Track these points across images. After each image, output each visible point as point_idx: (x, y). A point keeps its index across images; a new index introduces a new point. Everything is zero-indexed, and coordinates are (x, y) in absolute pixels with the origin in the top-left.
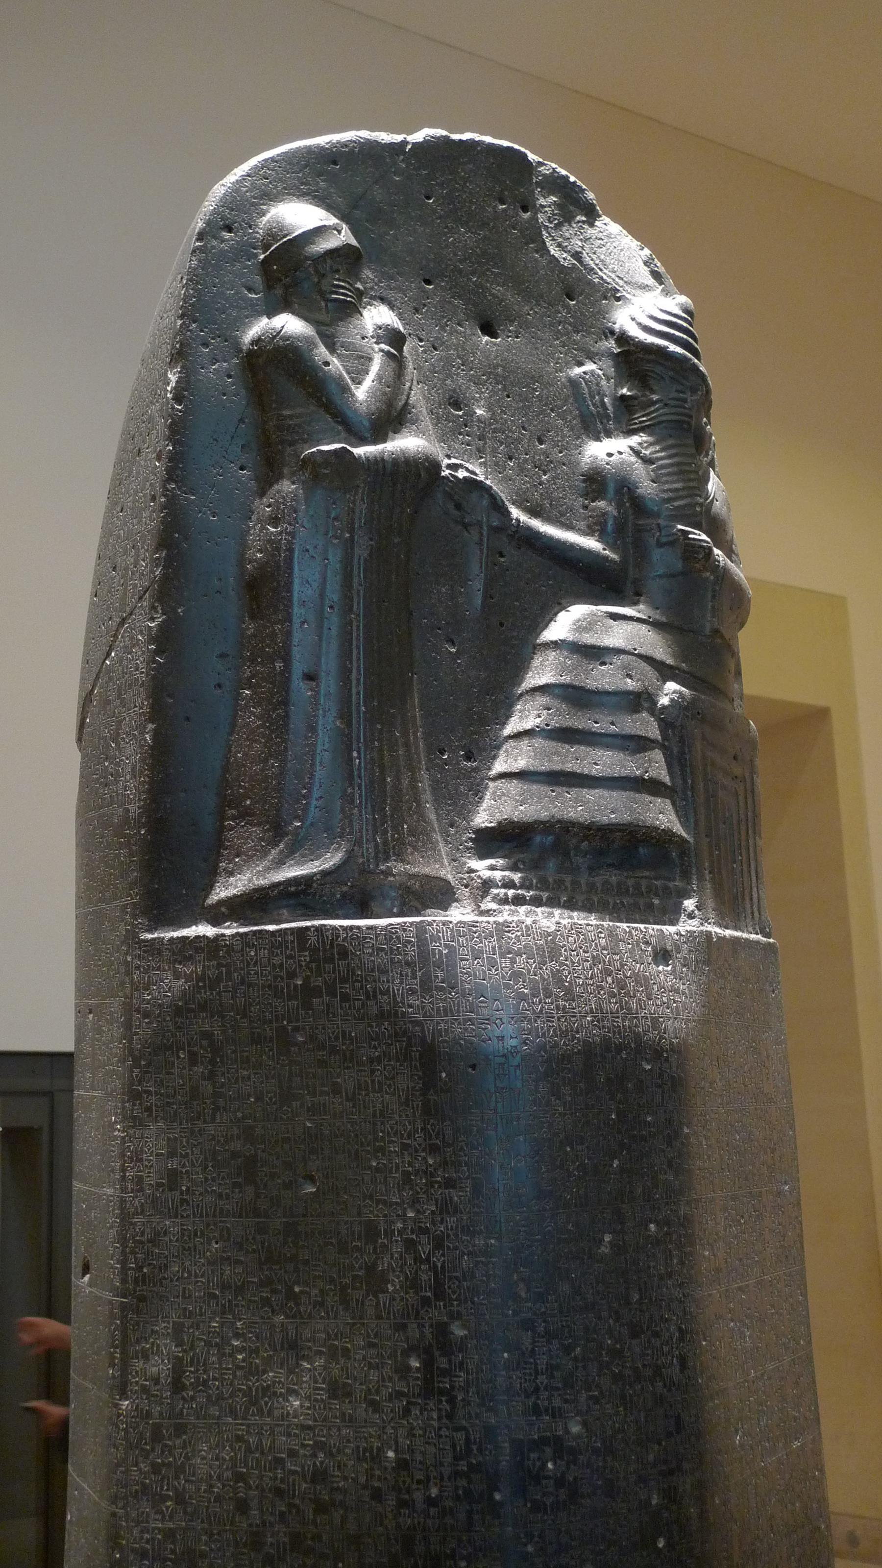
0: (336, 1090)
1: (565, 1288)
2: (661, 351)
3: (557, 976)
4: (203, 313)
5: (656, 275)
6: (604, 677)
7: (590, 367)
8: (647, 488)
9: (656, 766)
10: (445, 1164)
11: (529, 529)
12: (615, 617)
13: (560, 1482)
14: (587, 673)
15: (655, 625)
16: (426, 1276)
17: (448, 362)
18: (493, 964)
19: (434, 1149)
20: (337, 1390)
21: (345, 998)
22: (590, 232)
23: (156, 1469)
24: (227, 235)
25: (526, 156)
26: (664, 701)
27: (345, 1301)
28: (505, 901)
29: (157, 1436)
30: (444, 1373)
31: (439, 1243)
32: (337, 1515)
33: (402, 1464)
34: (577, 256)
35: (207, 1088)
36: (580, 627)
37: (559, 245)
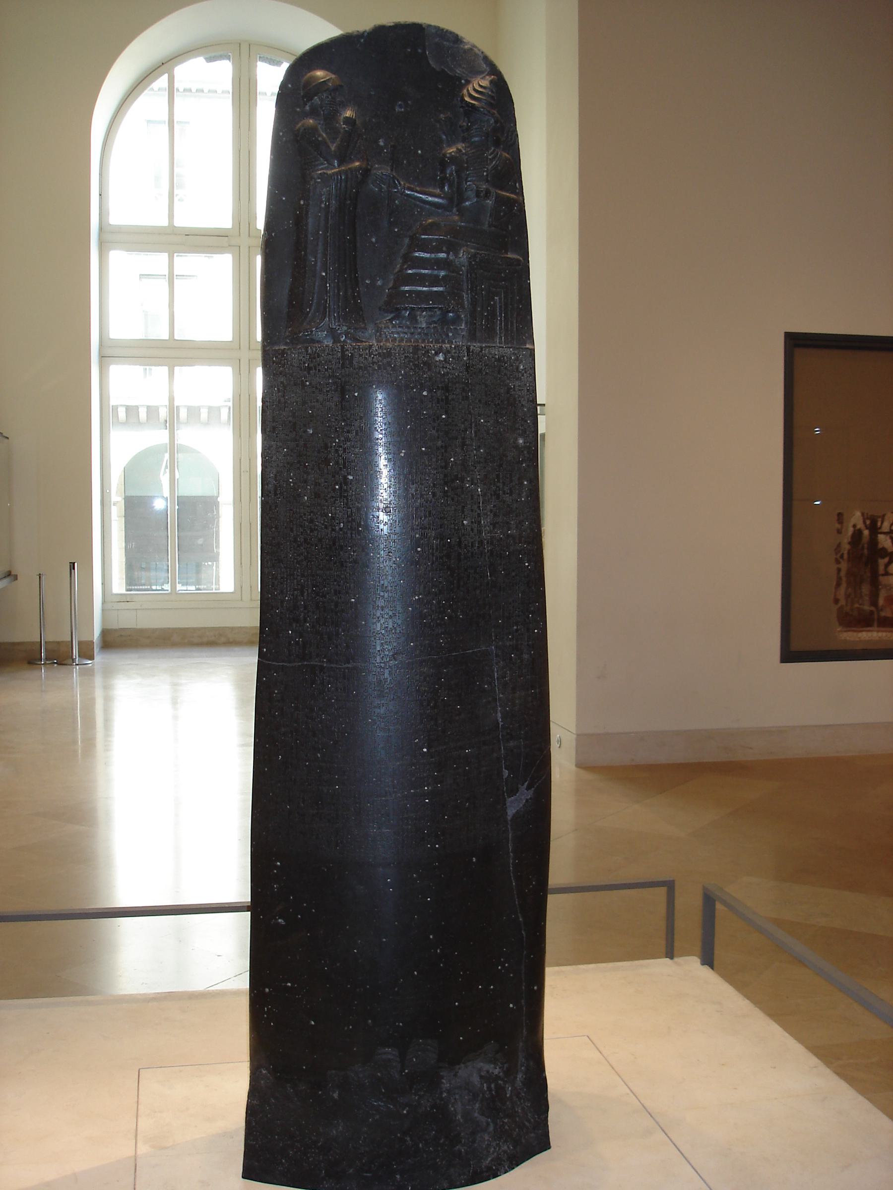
0: (317, 401)
3: (389, 364)
10: (346, 425)
16: (341, 461)
19: (344, 421)
20: (317, 495)
21: (319, 371)
23: (270, 519)
29: (270, 509)
30: (346, 491)
31: (345, 450)
32: (316, 532)
33: (333, 518)
35: (282, 399)
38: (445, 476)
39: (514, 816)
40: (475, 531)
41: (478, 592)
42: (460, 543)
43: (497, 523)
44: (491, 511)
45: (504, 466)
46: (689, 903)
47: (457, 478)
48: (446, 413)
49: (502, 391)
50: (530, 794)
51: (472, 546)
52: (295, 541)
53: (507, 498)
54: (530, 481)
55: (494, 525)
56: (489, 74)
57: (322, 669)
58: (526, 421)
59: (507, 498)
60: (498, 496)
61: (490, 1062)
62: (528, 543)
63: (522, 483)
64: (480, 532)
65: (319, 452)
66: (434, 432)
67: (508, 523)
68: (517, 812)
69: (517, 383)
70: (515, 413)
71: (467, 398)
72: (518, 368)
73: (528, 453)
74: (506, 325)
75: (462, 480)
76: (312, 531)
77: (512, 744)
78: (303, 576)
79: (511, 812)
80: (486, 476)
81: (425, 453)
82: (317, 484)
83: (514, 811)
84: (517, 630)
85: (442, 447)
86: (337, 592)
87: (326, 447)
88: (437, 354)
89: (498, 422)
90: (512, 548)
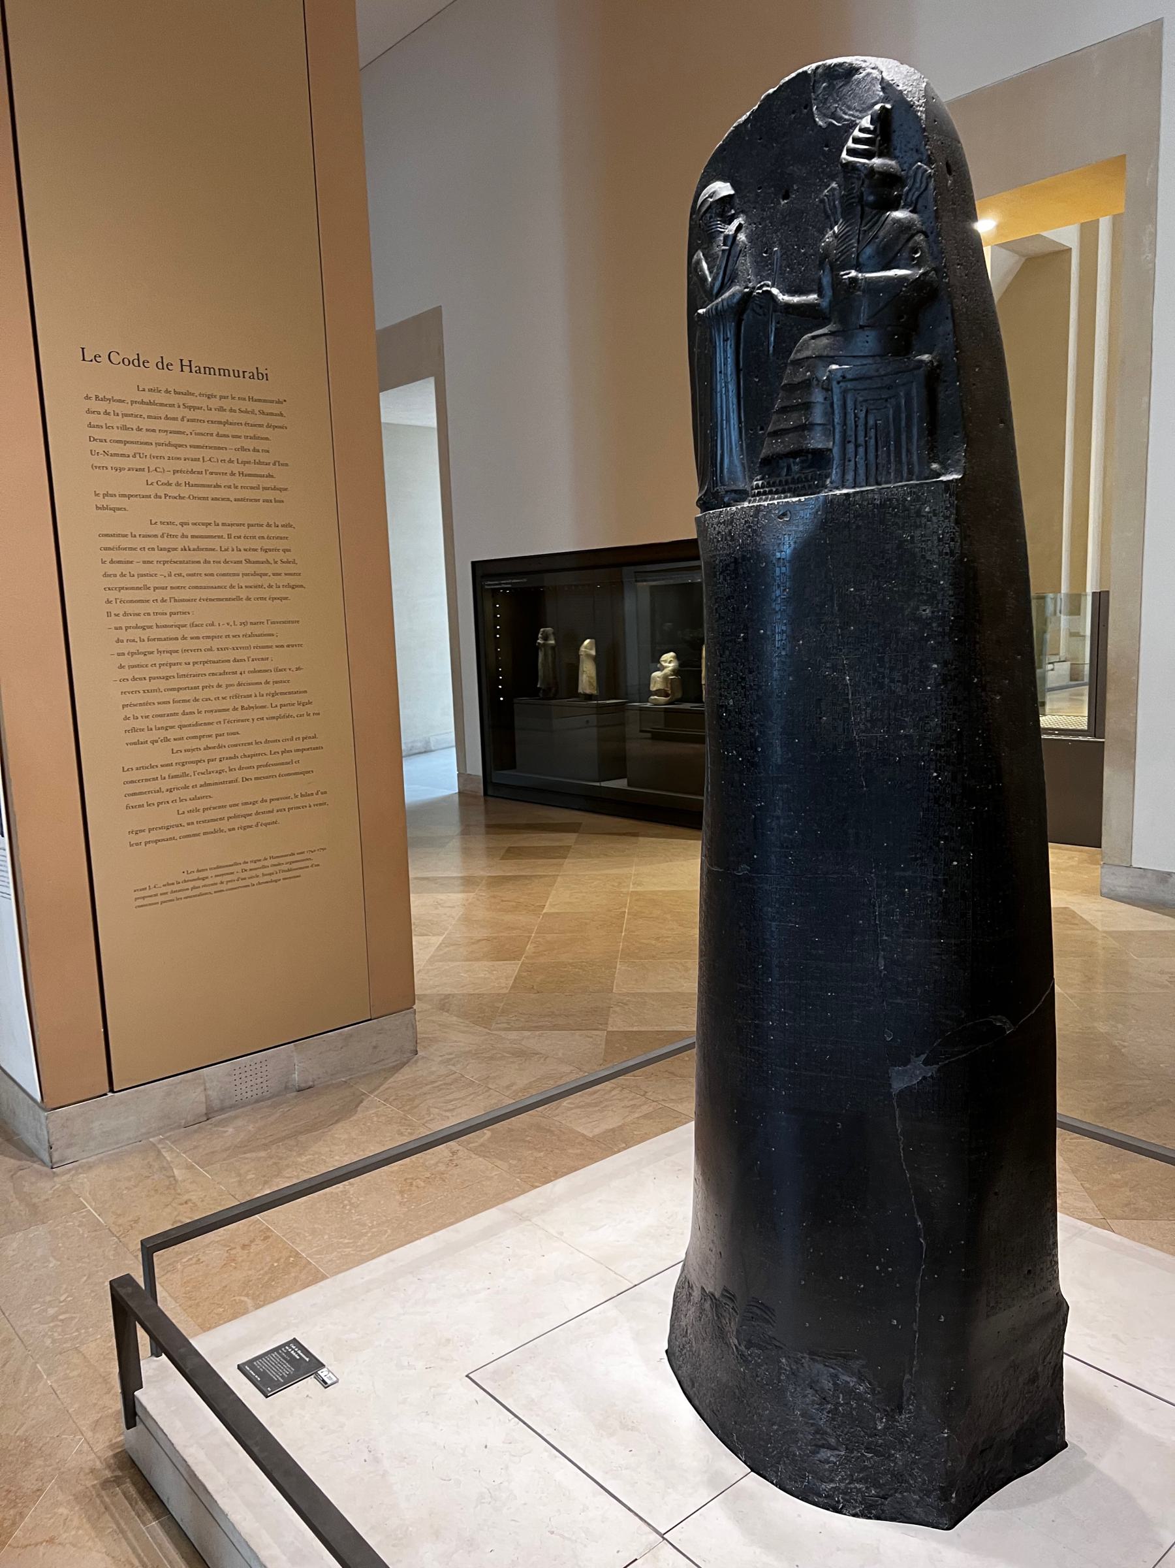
1: (727, 653)
12: (814, 338)
17: (764, 228)
37: (825, 116)
39: (902, 1091)
44: (867, 704)
45: (893, 646)
49: (888, 547)
50: (931, 1071)
51: (835, 748)
58: (937, 583)
59: (899, 689)
60: (881, 686)
61: (853, 1374)
63: (928, 667)
68: (909, 1088)
69: (918, 533)
73: (939, 625)
79: (897, 1085)
89: (880, 588)
90: (904, 753)
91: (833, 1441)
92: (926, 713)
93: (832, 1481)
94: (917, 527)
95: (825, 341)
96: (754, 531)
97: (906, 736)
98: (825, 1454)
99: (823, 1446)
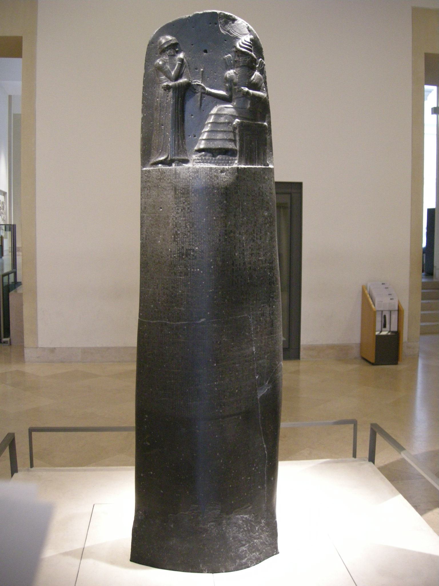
2: (241, 51)
3: (197, 176)
4: (149, 59)
5: (250, 31)
6: (222, 120)
7: (229, 55)
8: (236, 80)
9: (231, 136)
11: (210, 92)
12: (226, 107)
13: (193, 256)
14: (218, 119)
15: (235, 108)
18: (186, 174)
20: (164, 240)
22: (233, 25)
24: (153, 44)
25: (216, 13)
26: (234, 123)
27: (165, 227)
28: (197, 162)
33: (171, 251)
34: (228, 31)
36: (220, 110)
37: (224, 30)
38: (226, 231)
39: (261, 397)
40: (241, 258)
41: (243, 287)
42: (233, 264)
43: (253, 254)
44: (250, 248)
46: (364, 436)
47: (231, 231)
48: (226, 200)
52: (154, 262)
53: (259, 242)
54: (271, 233)
55: (252, 254)
56: (250, 34)
57: (166, 324)
58: (269, 203)
59: (259, 242)
60: (254, 241)
62: (270, 263)
63: (267, 234)
64: (244, 258)
65: (165, 219)
66: (219, 210)
67: (259, 253)
69: (264, 185)
70: (263, 199)
71: (237, 193)
72: (264, 178)
74: (258, 156)
75: (234, 233)
76: (162, 257)
77: (260, 362)
78: (158, 279)
80: (247, 231)
81: (215, 220)
82: (164, 235)
83: (261, 395)
84: (263, 306)
85: (224, 217)
86: (173, 287)
87: (168, 217)
88: (222, 172)
91: (244, 543)
92: (266, 251)
93: (246, 557)
94: (264, 183)
95: (233, 110)
96: (211, 177)
97: (261, 260)
98: (244, 548)
99: (241, 546)
